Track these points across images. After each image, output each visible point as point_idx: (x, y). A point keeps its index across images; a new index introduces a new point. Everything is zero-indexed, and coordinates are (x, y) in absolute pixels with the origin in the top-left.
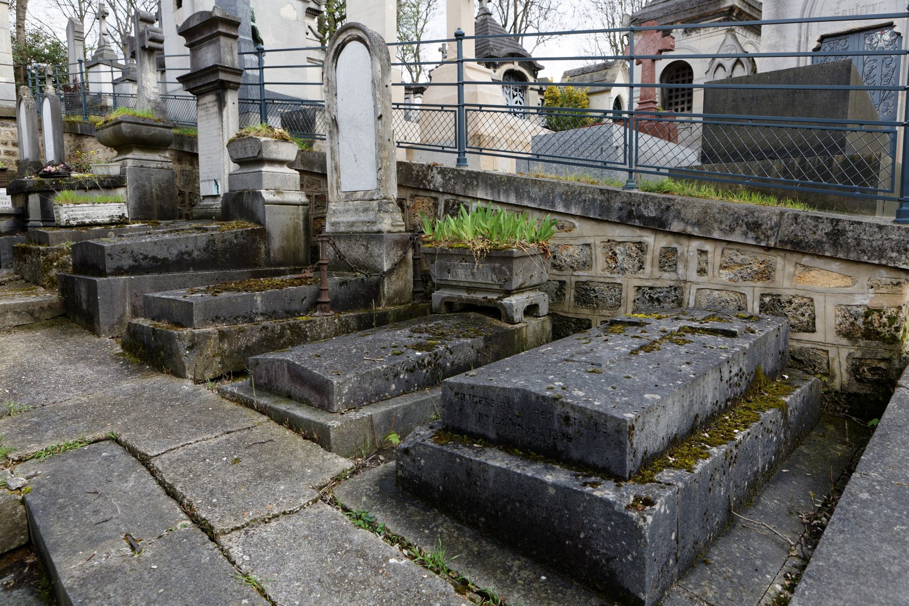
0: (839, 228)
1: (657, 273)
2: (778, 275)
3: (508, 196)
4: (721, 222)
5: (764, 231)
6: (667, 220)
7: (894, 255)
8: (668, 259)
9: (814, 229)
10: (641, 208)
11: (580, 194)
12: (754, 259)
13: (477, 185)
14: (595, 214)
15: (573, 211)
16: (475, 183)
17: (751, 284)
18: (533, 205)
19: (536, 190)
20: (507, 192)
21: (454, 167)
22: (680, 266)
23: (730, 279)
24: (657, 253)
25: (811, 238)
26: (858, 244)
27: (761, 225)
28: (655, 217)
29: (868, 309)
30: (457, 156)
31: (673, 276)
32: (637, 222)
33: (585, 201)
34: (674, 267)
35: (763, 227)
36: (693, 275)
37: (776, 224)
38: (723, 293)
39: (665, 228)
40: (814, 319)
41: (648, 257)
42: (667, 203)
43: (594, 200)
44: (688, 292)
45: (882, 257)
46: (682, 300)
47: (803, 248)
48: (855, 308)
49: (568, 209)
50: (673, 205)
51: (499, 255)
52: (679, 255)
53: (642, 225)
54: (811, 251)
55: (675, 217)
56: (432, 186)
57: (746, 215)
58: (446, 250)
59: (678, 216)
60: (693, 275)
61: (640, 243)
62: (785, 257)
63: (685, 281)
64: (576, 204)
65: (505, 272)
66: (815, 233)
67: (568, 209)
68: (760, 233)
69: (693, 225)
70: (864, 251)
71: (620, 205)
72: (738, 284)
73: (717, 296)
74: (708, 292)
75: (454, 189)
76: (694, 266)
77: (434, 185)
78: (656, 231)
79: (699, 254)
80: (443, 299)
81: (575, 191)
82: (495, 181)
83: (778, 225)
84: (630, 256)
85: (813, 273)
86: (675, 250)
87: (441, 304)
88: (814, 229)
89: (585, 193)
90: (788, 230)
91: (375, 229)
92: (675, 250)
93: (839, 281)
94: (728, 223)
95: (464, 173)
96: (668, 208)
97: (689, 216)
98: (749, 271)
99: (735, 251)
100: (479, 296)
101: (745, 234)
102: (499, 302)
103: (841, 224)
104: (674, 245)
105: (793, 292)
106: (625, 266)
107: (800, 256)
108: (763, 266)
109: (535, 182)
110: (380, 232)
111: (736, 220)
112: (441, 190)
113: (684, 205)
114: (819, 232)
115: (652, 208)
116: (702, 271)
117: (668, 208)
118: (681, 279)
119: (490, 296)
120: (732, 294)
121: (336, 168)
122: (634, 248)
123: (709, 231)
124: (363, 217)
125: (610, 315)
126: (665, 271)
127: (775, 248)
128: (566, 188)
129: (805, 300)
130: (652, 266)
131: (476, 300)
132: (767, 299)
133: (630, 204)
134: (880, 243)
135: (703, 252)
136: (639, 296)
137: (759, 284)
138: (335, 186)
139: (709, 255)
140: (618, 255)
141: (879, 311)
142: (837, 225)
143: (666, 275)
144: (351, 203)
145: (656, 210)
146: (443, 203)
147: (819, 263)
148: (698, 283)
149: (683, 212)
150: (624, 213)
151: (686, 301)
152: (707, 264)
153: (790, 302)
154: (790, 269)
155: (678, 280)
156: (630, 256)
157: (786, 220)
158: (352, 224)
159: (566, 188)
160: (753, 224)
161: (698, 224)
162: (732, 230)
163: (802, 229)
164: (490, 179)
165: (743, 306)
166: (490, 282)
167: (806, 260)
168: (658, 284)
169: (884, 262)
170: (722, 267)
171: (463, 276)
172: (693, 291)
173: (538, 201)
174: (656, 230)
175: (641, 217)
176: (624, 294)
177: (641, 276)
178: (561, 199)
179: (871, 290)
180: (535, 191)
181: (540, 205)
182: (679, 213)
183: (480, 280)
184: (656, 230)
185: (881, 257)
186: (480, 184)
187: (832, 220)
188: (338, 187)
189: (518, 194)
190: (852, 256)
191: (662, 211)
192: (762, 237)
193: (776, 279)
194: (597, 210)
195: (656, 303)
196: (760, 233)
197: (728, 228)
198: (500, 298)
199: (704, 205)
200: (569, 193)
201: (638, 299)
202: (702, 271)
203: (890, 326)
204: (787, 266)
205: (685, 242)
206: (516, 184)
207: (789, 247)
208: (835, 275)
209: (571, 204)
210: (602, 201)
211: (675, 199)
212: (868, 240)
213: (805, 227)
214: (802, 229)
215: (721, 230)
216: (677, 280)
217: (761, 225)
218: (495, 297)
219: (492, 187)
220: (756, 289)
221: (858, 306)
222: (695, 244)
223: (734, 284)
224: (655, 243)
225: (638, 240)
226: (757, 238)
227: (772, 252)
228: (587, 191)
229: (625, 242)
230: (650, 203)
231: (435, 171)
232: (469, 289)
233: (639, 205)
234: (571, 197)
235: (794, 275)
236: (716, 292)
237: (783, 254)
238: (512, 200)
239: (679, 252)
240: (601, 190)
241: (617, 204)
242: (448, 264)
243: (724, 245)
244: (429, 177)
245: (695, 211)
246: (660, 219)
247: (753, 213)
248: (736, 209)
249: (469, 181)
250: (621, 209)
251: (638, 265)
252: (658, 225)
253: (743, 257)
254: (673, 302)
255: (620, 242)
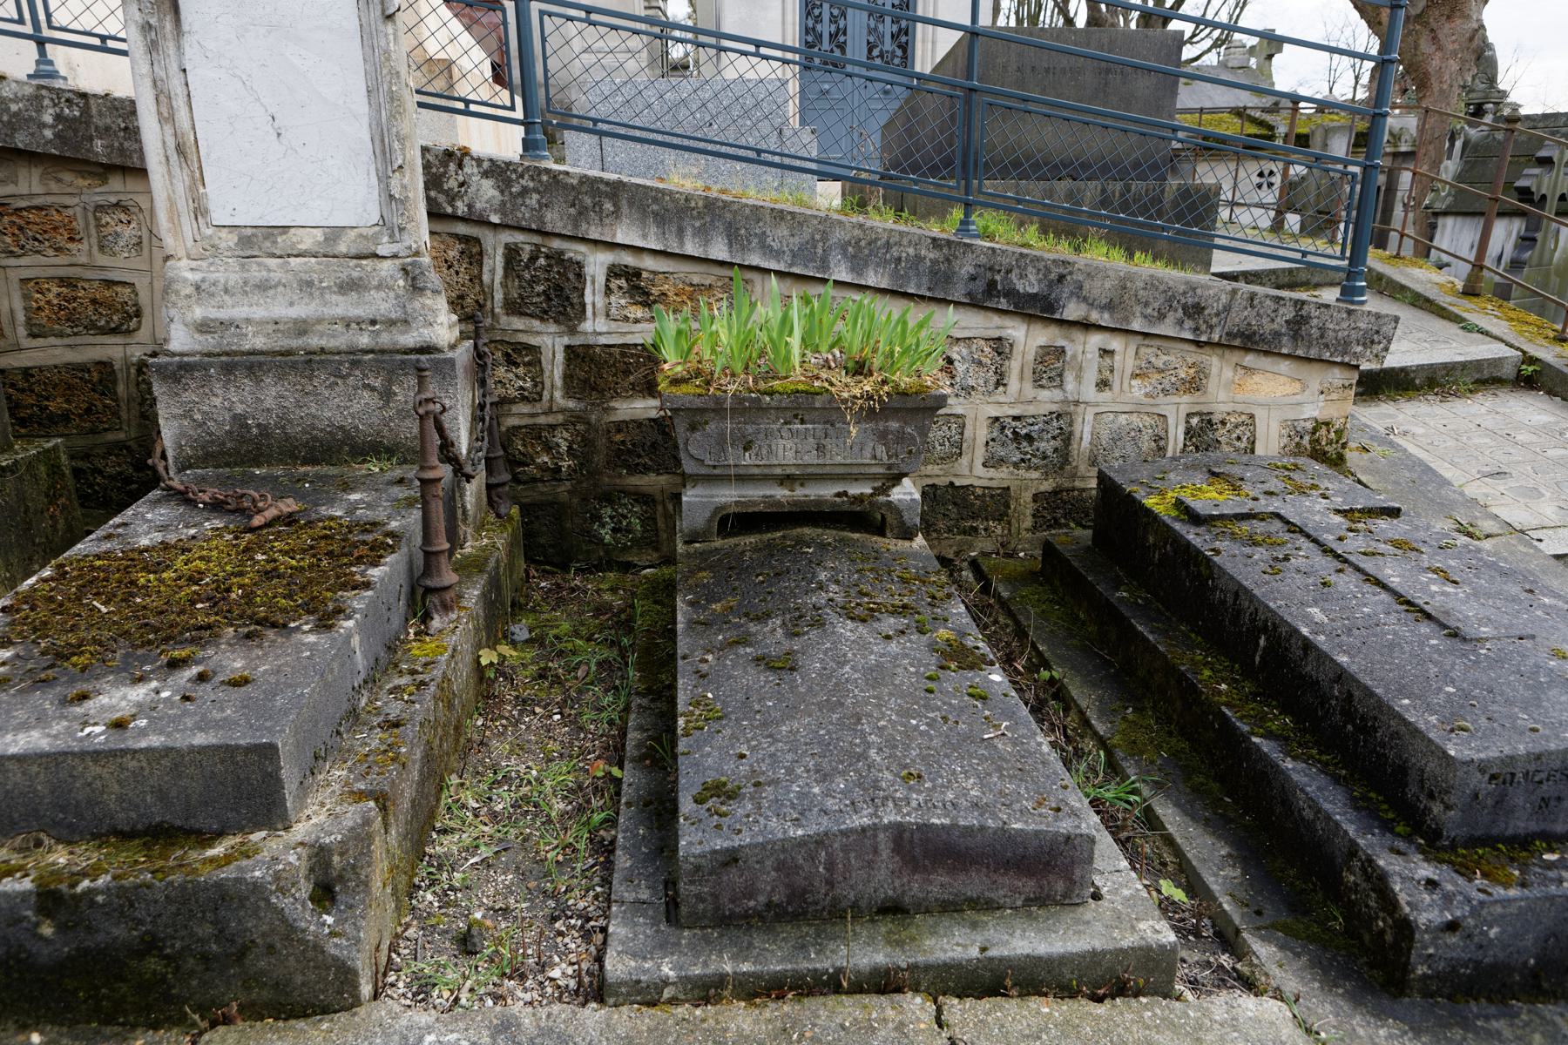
0: (1303, 313)
1: (1029, 391)
2: (1212, 385)
3: (706, 243)
4: (1146, 304)
5: (1207, 318)
6: (1057, 300)
7: (1359, 349)
8: (1050, 366)
9: (1273, 315)
10: (1013, 276)
11: (888, 245)
12: (1180, 361)
13: (616, 213)
14: (919, 286)
15: (871, 279)
16: (608, 206)
17: (1175, 399)
18: (773, 265)
19: (783, 231)
20: (703, 234)
21: (517, 159)
22: (1069, 377)
23: (1147, 395)
24: (1031, 357)
25: (1268, 327)
26: (1322, 336)
27: (1203, 308)
28: (1036, 294)
29: (1316, 421)
30: (519, 131)
31: (1057, 394)
32: (1003, 304)
33: (899, 259)
34: (1058, 380)
35: (1206, 312)
36: (1089, 392)
37: (1224, 307)
38: (1134, 418)
39: (1053, 313)
40: (1254, 442)
41: (1014, 365)
42: (1061, 270)
43: (919, 259)
44: (1080, 420)
45: (1346, 353)
46: (1071, 434)
47: (1256, 343)
48: (1302, 424)
49: (860, 275)
50: (1071, 273)
51: (909, 405)
52: (1068, 358)
53: (1011, 308)
54: (1266, 348)
55: (1072, 293)
56: (461, 208)
57: (1184, 293)
58: (752, 400)
59: (1078, 293)
60: (1089, 392)
61: (1000, 339)
62: (1222, 357)
63: (1077, 403)
64: (878, 265)
65: (913, 438)
66: (1273, 320)
67: (860, 275)
68: (1201, 322)
69: (1103, 308)
70: (1327, 346)
71: (972, 270)
72: (1158, 401)
73: (1124, 422)
74: (1112, 415)
75: (541, 219)
76: (1091, 376)
77: (470, 206)
78: (1030, 318)
79: (1101, 356)
80: (718, 509)
81: (877, 239)
82: (671, 206)
83: (1227, 309)
84: (980, 363)
85: (1256, 378)
86: (1062, 351)
87: (710, 520)
88: (1273, 315)
89: (899, 244)
90: (1240, 316)
91: (409, 339)
92: (1062, 351)
93: (1287, 387)
94: (1156, 305)
95: (575, 182)
96: (1061, 278)
97: (1096, 292)
98: (1173, 379)
99: (1155, 350)
100: (827, 491)
101: (1180, 323)
102: (882, 498)
103: (1305, 307)
104: (1060, 342)
105: (1229, 408)
106: (971, 382)
107: (1242, 353)
108: (1192, 371)
109: (779, 215)
110: (427, 349)
111: (1170, 300)
112: (495, 219)
113: (1089, 274)
114: (1279, 320)
115: (1032, 278)
116: (1103, 384)
117: (1061, 278)
118: (1071, 398)
119: (855, 490)
120: (1146, 418)
121: (184, 151)
122: (987, 350)
123: (1127, 320)
124: (342, 306)
125: (941, 473)
126: (1042, 387)
127: (1219, 345)
128: (857, 232)
129: (1244, 417)
130: (1022, 379)
131: (819, 502)
132: (1195, 421)
133: (991, 269)
134: (1346, 333)
135: (1106, 352)
136: (995, 434)
137: (1186, 398)
138: (183, 206)
139: (1117, 358)
140: (956, 363)
141: (1327, 424)
142: (1301, 309)
143: (1044, 394)
144: (273, 262)
145: (1040, 281)
146: (500, 251)
147: (1265, 362)
148: (1097, 404)
149: (1086, 286)
150: (980, 286)
151: (1077, 435)
152: (1112, 371)
153: (1223, 423)
154: (1228, 373)
155: (1065, 401)
156: (980, 363)
157: (1240, 301)
158: (302, 327)
159: (857, 232)
160: (1193, 307)
161: (1110, 306)
162: (1162, 317)
163: (1258, 315)
164: (655, 200)
165: (1162, 434)
166: (868, 461)
167: (1250, 359)
168: (1031, 410)
169: (1347, 359)
170: (1135, 376)
171: (790, 454)
172: (1089, 417)
173: (787, 257)
174: (1030, 316)
175: (1011, 293)
176: (968, 433)
177: (1002, 399)
178: (845, 254)
179: (1322, 397)
180: (779, 235)
181: (791, 265)
182: (1081, 288)
183: (839, 459)
184: (1030, 316)
185: (1344, 353)
186: (625, 209)
187: (1296, 302)
188: (200, 211)
189: (733, 237)
190: (1313, 353)
191: (1051, 285)
192: (1204, 327)
193: (1210, 390)
194: (925, 280)
195: (1025, 444)
196: (1201, 322)
197: (1156, 314)
198: (884, 490)
199: (1122, 274)
200: (863, 243)
201: (993, 440)
202: (1103, 384)
203: (1337, 442)
204: (1224, 370)
205: (1078, 335)
206: (728, 216)
207: (1237, 342)
208: (1282, 379)
209: (866, 265)
210: (934, 262)
211: (1075, 263)
212: (1334, 330)
213: (1261, 311)
214: (1258, 315)
215: (1145, 317)
216: (1062, 402)
217: (1203, 308)
218: (869, 491)
219: (661, 219)
220: (1182, 407)
221: (1305, 420)
222: (1096, 340)
223: (1151, 401)
224: (1026, 338)
225: (996, 334)
226: (1196, 330)
227: (1207, 350)
228: (905, 241)
229: (970, 339)
230: (1030, 269)
231: (470, 168)
232: (787, 480)
233: (1009, 271)
234: (867, 252)
235: (1233, 382)
236: (1124, 416)
237: (1219, 351)
238: (719, 251)
239: (1069, 353)
240: (934, 240)
241: (965, 268)
242: (750, 429)
243: (1139, 338)
244: (452, 184)
245: (1107, 285)
246: (1045, 297)
247: (1194, 289)
248: (1171, 283)
249: (588, 201)
250: (973, 278)
251: (994, 379)
252: (1039, 309)
253: (1165, 358)
254: (1054, 438)
255: (958, 339)
